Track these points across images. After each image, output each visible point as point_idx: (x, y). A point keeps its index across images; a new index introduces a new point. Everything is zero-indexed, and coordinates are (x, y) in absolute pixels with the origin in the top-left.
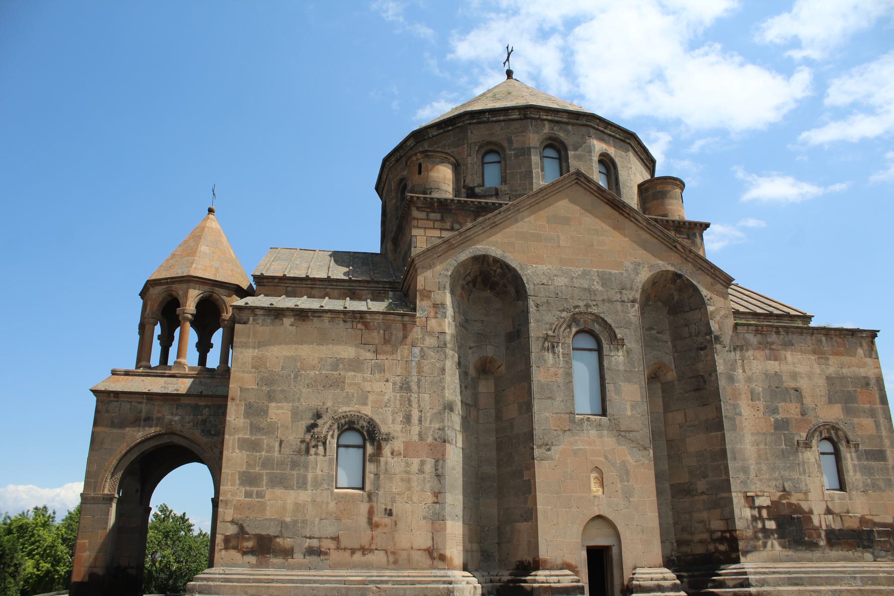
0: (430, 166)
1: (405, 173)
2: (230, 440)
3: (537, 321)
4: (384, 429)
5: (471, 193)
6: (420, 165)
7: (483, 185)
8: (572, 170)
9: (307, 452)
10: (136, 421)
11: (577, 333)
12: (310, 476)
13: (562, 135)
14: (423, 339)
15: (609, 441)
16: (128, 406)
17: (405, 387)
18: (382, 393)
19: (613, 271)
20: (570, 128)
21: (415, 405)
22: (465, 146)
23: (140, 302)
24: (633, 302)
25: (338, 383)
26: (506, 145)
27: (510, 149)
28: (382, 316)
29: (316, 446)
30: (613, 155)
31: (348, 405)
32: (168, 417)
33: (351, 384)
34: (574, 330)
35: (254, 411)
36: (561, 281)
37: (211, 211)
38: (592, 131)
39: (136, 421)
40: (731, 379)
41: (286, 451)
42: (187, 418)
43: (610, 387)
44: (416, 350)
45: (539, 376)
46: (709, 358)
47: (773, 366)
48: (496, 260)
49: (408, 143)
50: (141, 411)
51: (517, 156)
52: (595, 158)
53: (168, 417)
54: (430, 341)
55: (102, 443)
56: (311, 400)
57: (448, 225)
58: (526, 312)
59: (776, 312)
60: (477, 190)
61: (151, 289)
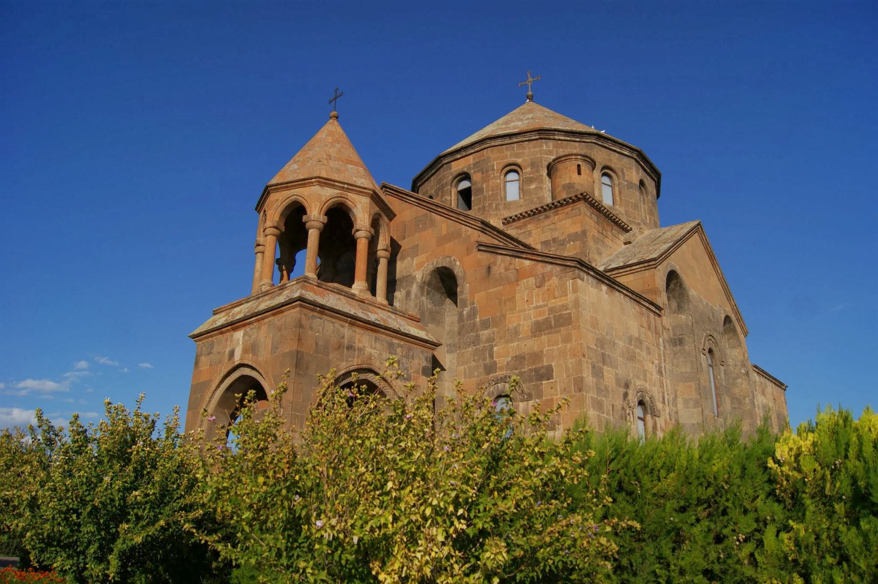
6: (579, 166)
10: (339, 347)
13: (646, 182)
16: (331, 325)
17: (660, 372)
25: (632, 358)
26: (620, 174)
28: (647, 305)
29: (629, 414)
31: (639, 378)
32: (368, 350)
33: (639, 361)
35: (598, 373)
39: (339, 347)
42: (385, 355)
46: (744, 386)
50: (343, 337)
51: (628, 188)
53: (368, 350)
55: (307, 368)
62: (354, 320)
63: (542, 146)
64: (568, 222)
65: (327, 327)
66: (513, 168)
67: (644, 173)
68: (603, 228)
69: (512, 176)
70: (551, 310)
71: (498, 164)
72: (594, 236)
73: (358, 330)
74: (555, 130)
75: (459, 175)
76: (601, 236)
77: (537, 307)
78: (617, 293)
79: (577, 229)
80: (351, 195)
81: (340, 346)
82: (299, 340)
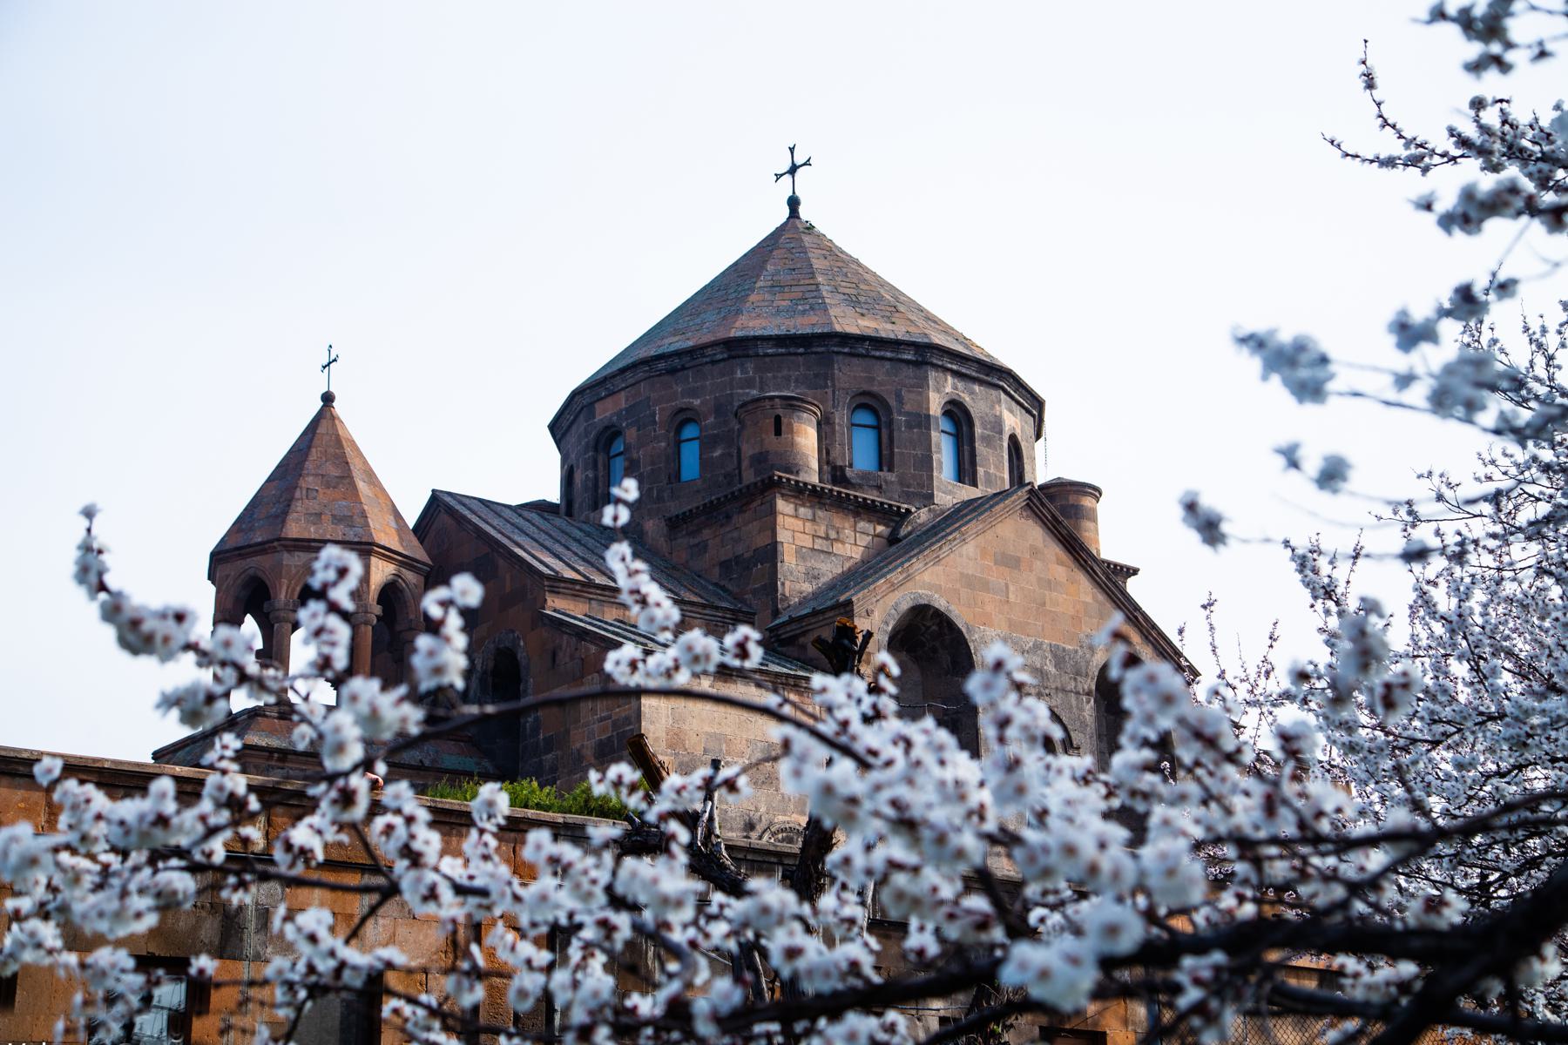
0: (796, 425)
1: (697, 402)
6: (778, 420)
7: (851, 465)
13: (967, 399)
19: (1068, 647)
20: (976, 388)
22: (829, 391)
24: (1088, 694)
26: (893, 403)
27: (900, 413)
38: (1003, 396)
49: (709, 351)
52: (1006, 445)
57: (822, 532)
61: (286, 555)
63: (733, 372)
64: (754, 526)
66: (684, 417)
67: (960, 385)
68: (830, 526)
69: (690, 431)
70: (615, 724)
71: (662, 410)
72: (799, 549)
74: (756, 338)
75: (607, 428)
77: (602, 720)
79: (762, 541)
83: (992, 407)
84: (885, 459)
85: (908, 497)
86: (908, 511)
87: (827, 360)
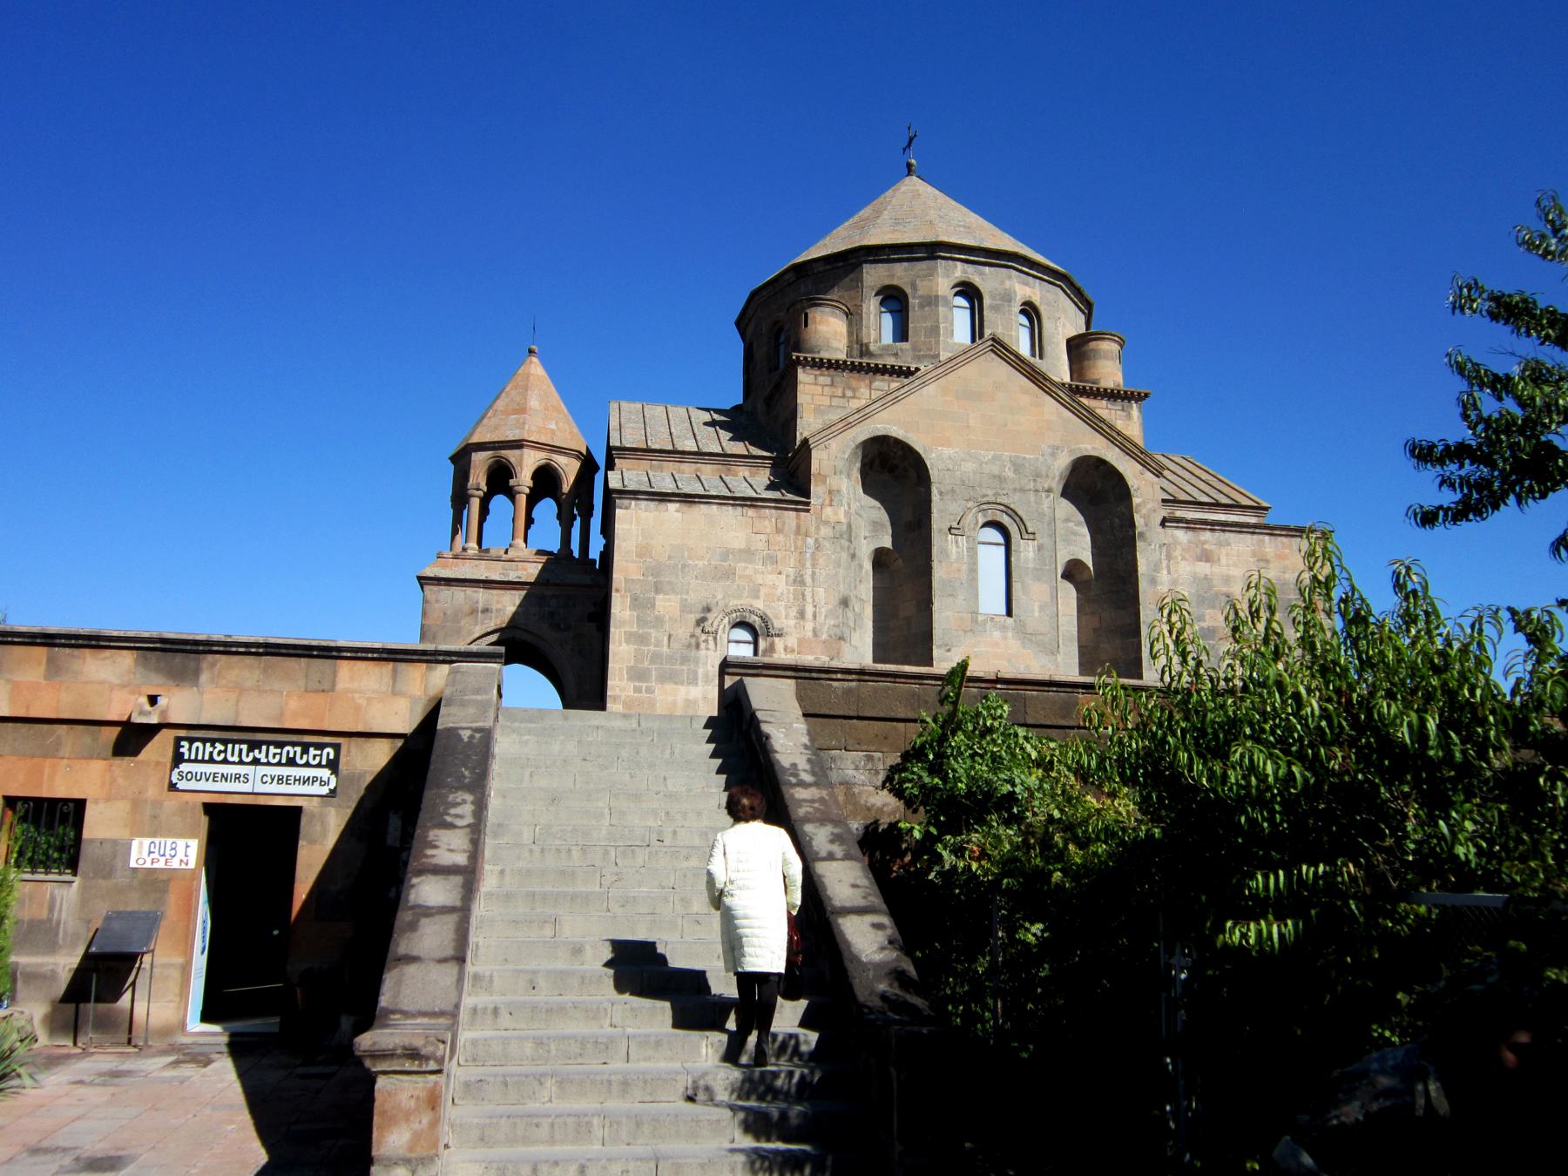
0: (818, 318)
2: (616, 633)
3: (941, 511)
4: (777, 624)
5: (864, 350)
8: (987, 332)
9: (698, 646)
11: (984, 525)
12: (701, 671)
13: (976, 280)
14: (818, 528)
15: (1014, 645)
17: (799, 581)
18: (774, 586)
20: (987, 269)
21: (809, 599)
23: (450, 468)
25: (729, 574)
26: (908, 291)
29: (706, 641)
30: (1037, 303)
31: (739, 597)
34: (981, 521)
36: (969, 467)
37: (531, 352)
38: (1014, 272)
40: (1153, 581)
41: (675, 645)
43: (1016, 587)
44: (810, 541)
45: (939, 573)
47: (1203, 568)
48: (897, 442)
51: (922, 306)
54: (825, 531)
56: (698, 593)
57: (839, 392)
58: (930, 501)
59: (1225, 500)
60: (872, 348)
62: (488, 584)
65: (459, 593)
67: (970, 268)
69: (782, 338)
73: (495, 592)
76: (835, 402)
78: (702, 506)
80: (503, 453)
81: (473, 612)
82: (424, 614)
83: (1002, 282)
84: (901, 333)
85: (919, 358)
86: (917, 369)
87: (857, 266)
